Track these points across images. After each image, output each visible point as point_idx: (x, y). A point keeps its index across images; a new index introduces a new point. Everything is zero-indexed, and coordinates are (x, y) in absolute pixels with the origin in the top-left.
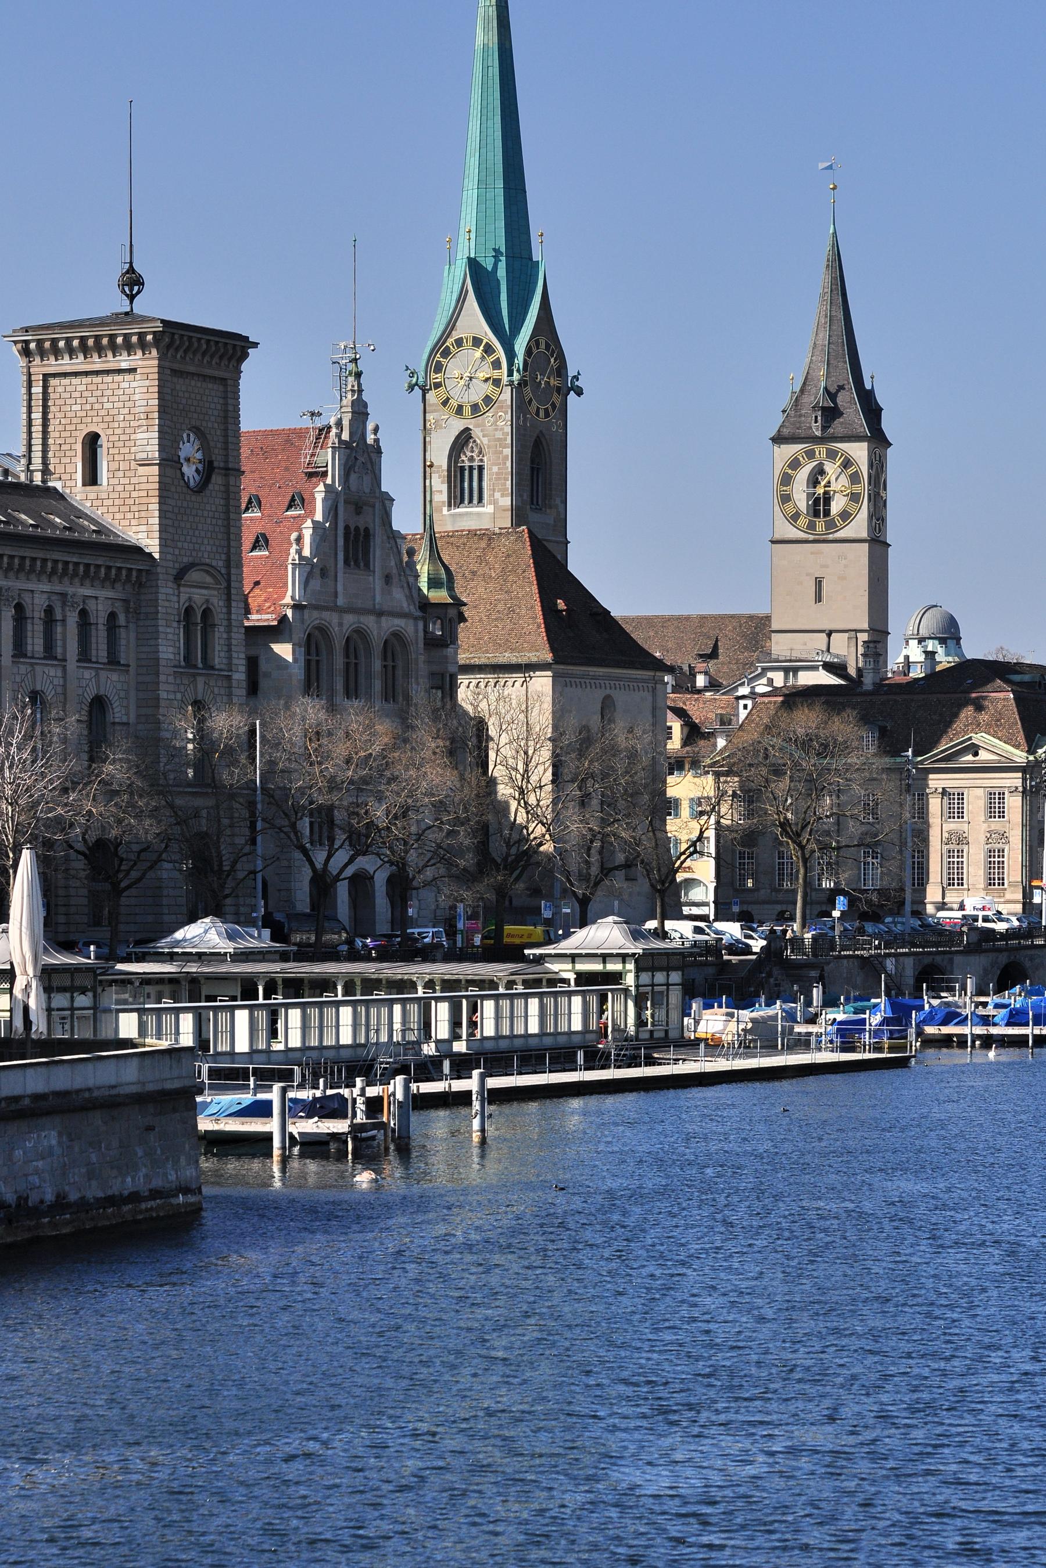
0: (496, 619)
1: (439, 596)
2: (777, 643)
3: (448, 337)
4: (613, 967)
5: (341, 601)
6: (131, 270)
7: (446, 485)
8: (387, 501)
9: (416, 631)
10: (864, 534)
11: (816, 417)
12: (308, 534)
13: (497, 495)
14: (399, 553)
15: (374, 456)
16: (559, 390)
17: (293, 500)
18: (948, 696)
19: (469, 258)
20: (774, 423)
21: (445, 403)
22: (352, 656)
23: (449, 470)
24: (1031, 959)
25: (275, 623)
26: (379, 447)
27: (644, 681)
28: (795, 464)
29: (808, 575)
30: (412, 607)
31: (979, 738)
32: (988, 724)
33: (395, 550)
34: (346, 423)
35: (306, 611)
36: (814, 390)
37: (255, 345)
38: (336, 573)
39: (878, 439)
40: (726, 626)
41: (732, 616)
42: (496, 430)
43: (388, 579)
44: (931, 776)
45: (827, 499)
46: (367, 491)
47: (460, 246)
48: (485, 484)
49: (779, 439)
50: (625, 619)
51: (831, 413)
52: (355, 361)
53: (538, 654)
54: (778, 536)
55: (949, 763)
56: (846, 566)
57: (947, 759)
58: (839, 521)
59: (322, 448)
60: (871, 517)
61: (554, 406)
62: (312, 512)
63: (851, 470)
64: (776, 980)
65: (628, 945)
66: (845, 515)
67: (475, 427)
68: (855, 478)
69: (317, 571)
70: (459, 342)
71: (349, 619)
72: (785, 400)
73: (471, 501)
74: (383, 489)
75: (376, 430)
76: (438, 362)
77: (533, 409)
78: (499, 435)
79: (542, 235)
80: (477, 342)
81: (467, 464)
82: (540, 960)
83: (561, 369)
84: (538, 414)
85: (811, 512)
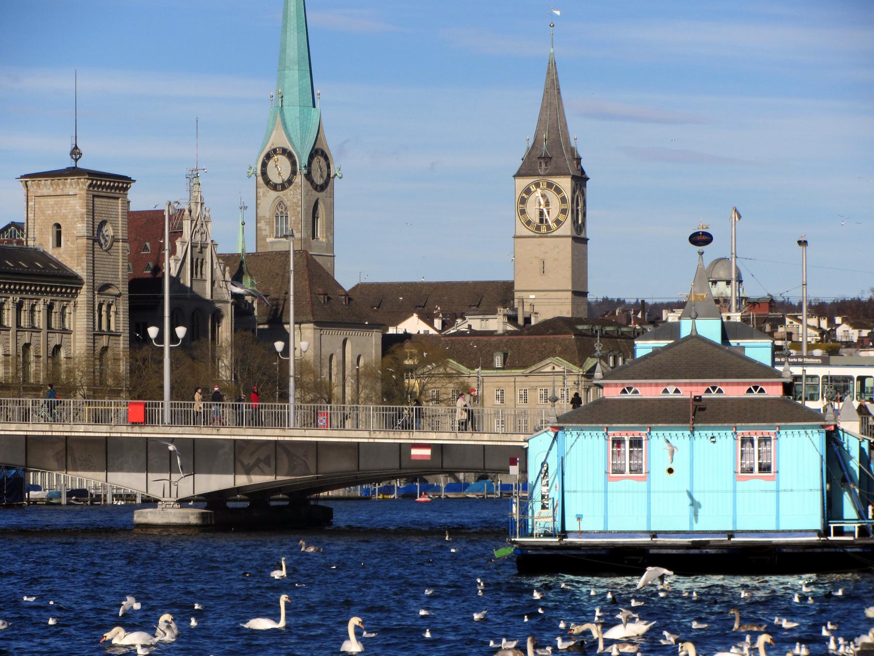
6: (76, 147)
11: (541, 163)
28: (528, 191)
37: (134, 181)
56: (558, 253)
66: (558, 222)
67: (284, 195)
68: (563, 200)
78: (295, 200)
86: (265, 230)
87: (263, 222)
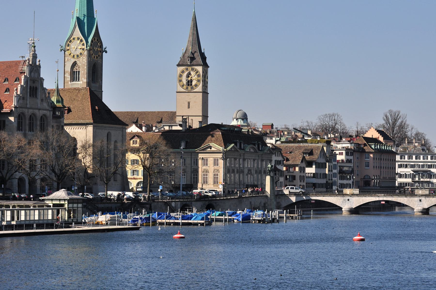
0: (79, 111)
1: (59, 105)
2: (178, 119)
3: (71, 37)
4: (62, 202)
5: (28, 106)
7: (70, 76)
8: (42, 80)
9: (50, 114)
10: (201, 90)
11: (189, 60)
12: (19, 88)
13: (83, 79)
14: (45, 94)
15: (38, 68)
16: (100, 51)
17: (16, 79)
18: (204, 133)
19: (77, 17)
20: (178, 61)
21: (70, 54)
22: (32, 120)
23: (71, 72)
24: (216, 203)
25: (9, 111)
26: (40, 66)
27: (119, 128)
28: (183, 72)
29: (186, 101)
30: (49, 108)
31: (211, 144)
32: (214, 141)
33: (44, 93)
34: (31, 59)
35: (18, 109)
36: (188, 53)
38: (27, 98)
39: (205, 65)
40: (165, 114)
41: (167, 112)
42: (83, 62)
43: (42, 100)
44: (199, 154)
45: (191, 81)
46: (36, 77)
47: (75, 14)
48: (80, 76)
49: (179, 65)
50: (116, 112)
51: (192, 59)
52: (34, 43)
53: (89, 121)
54: (178, 91)
55: (204, 151)
56: (196, 99)
57: (203, 150)
58: (194, 87)
59: (25, 66)
60: (203, 86)
61: (99, 56)
62: (21, 82)
63: (198, 74)
64: (137, 207)
65: (66, 197)
66: (196, 85)
67: (78, 61)
68: (199, 76)
69: (22, 98)
70: (74, 39)
71: (31, 111)
72: (181, 55)
73: (76, 80)
74: (41, 77)
75: (39, 61)
76: (68, 44)
77: (93, 56)
78: (84, 63)
79: (96, 11)
80: (78, 39)
81: (75, 70)
82: (43, 200)
83: (101, 46)
84: (94, 58)
85: (187, 84)
86: (68, 78)
87: (67, 74)
